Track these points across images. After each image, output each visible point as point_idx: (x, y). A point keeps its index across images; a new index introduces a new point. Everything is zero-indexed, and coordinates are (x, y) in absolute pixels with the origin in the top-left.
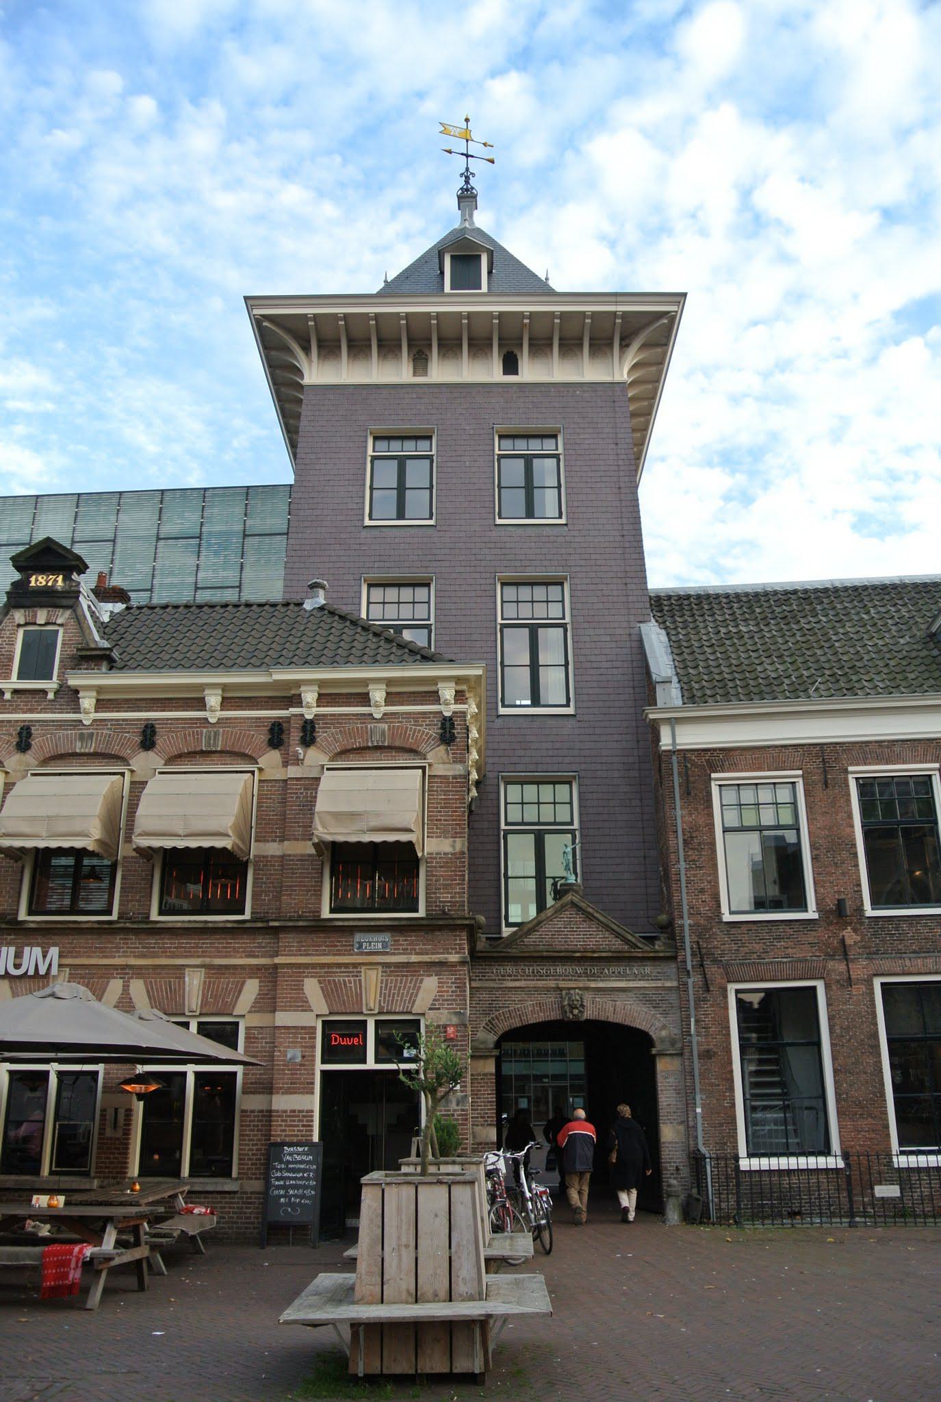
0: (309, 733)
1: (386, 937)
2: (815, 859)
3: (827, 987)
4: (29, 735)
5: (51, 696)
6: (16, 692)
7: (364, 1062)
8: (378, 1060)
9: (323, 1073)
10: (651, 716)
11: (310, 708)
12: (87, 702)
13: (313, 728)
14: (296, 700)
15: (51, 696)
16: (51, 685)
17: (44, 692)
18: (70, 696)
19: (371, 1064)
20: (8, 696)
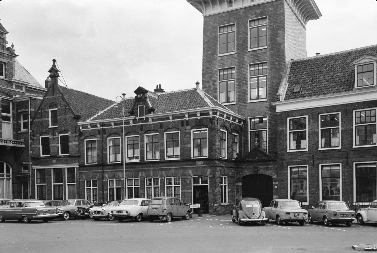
0: (187, 123)
1: (202, 162)
2: (309, 136)
3: (309, 166)
4: (142, 127)
5: (144, 119)
6: (139, 119)
7: (199, 184)
8: (202, 184)
9: (193, 186)
10: (273, 104)
11: (187, 118)
12: (150, 120)
13: (188, 122)
14: (184, 117)
15: (144, 119)
16: (144, 117)
17: (143, 119)
18: (147, 119)
19: (200, 184)
20: (138, 120)
